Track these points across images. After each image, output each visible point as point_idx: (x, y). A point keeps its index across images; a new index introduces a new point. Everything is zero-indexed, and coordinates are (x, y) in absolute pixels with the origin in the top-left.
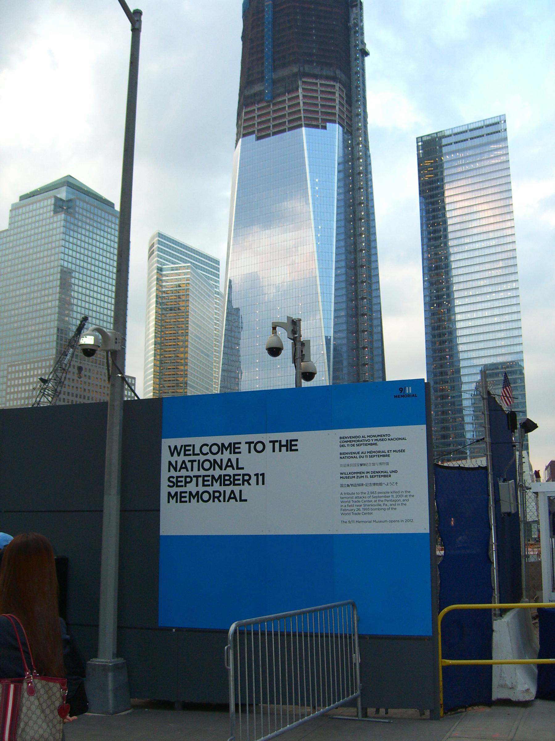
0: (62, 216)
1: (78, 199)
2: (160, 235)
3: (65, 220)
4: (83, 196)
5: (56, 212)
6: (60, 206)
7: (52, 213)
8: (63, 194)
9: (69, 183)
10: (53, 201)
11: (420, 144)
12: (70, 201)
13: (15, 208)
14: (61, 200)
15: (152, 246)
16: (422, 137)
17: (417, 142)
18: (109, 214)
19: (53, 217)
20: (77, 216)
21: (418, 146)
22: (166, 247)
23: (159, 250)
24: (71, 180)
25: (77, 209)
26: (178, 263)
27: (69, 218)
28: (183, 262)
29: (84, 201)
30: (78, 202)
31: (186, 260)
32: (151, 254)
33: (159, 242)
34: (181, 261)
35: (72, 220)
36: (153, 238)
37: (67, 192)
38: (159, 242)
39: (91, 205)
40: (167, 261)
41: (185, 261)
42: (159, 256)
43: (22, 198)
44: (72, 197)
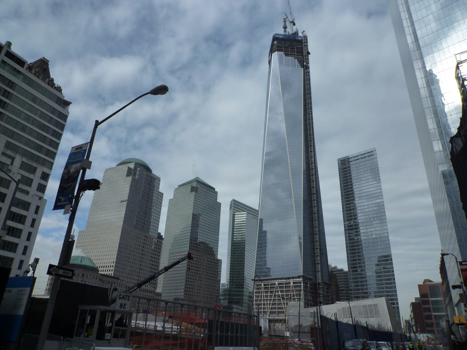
0: (194, 193)
3: (195, 195)
5: (191, 191)
6: (193, 189)
8: (195, 184)
9: (198, 181)
13: (176, 190)
14: (194, 187)
15: (231, 205)
22: (237, 206)
23: (234, 206)
24: (198, 179)
32: (230, 208)
36: (231, 202)
38: (234, 204)
42: (233, 209)
43: (179, 186)
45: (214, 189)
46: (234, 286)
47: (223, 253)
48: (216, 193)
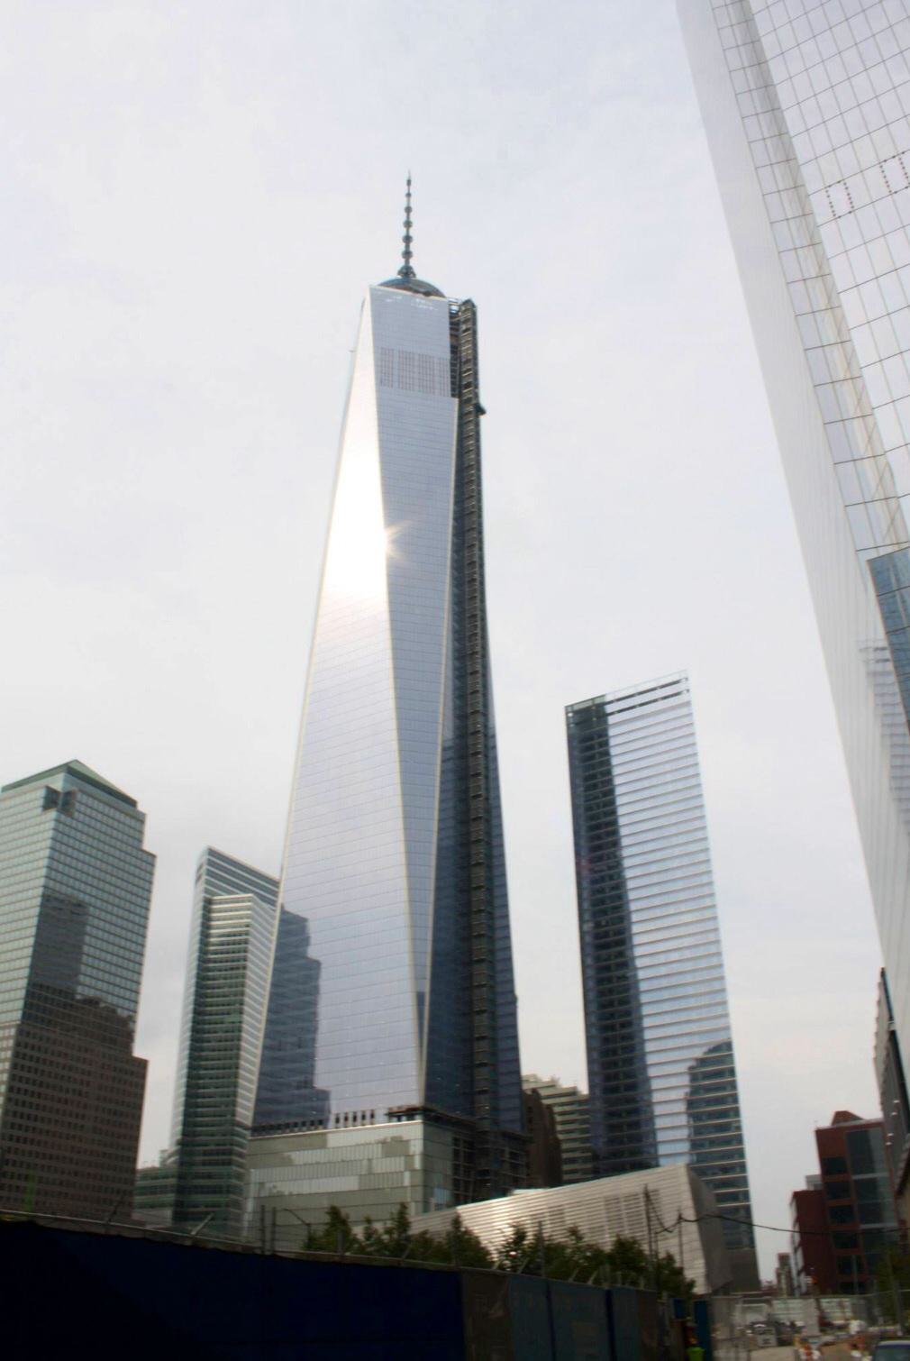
0: (53, 814)
1: (81, 791)
2: (212, 852)
3: (58, 821)
4: (90, 789)
6: (51, 800)
7: (39, 810)
8: (58, 783)
9: (73, 771)
10: (42, 793)
11: (570, 715)
12: (68, 794)
16: (572, 706)
17: (567, 713)
18: (127, 814)
19: (40, 815)
20: (76, 814)
21: (568, 718)
23: (210, 873)
24: (72, 765)
25: (77, 805)
26: (233, 893)
27: (63, 817)
28: (241, 890)
29: (90, 795)
30: (79, 796)
31: (246, 888)
32: (198, 878)
33: (210, 863)
34: (237, 888)
35: (68, 820)
37: (66, 781)
39: (100, 801)
40: (220, 890)
41: (245, 890)
44: (74, 788)
45: (133, 803)
46: (199, 1159)
47: (161, 1045)
48: (140, 819)
